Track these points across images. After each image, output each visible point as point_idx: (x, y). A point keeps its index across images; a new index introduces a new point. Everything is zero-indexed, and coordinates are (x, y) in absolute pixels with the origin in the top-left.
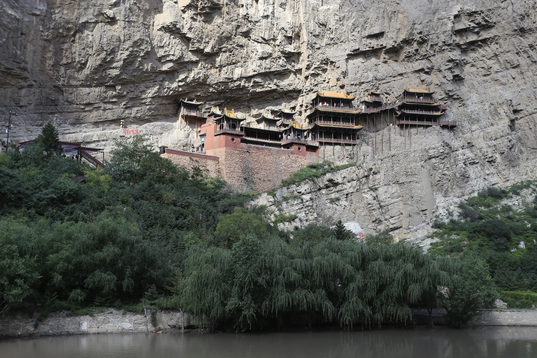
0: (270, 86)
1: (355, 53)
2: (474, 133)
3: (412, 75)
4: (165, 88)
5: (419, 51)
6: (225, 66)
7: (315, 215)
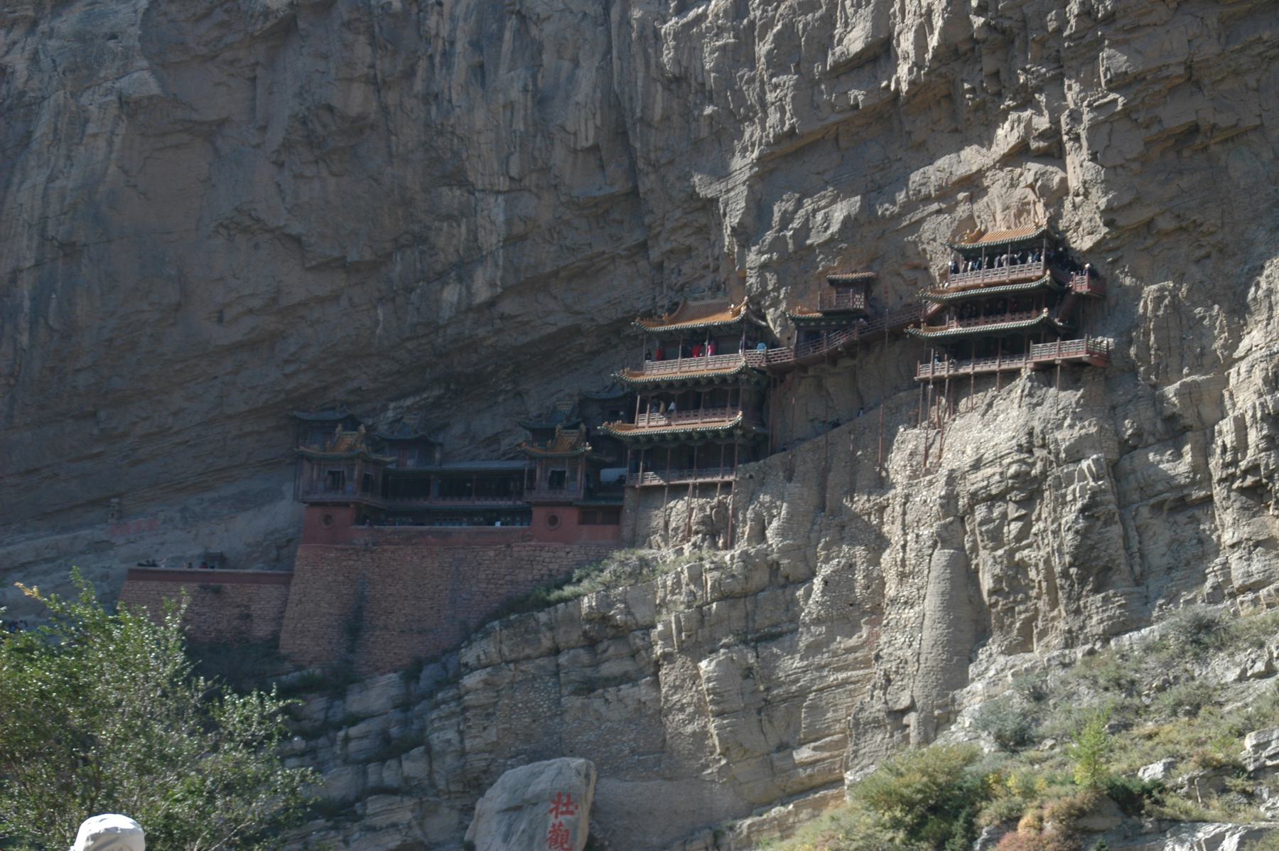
0: (551, 319)
1: (787, 147)
2: (1233, 371)
3: (1001, 174)
4: (242, 391)
5: (1003, 76)
6: (412, 290)
7: (492, 735)
